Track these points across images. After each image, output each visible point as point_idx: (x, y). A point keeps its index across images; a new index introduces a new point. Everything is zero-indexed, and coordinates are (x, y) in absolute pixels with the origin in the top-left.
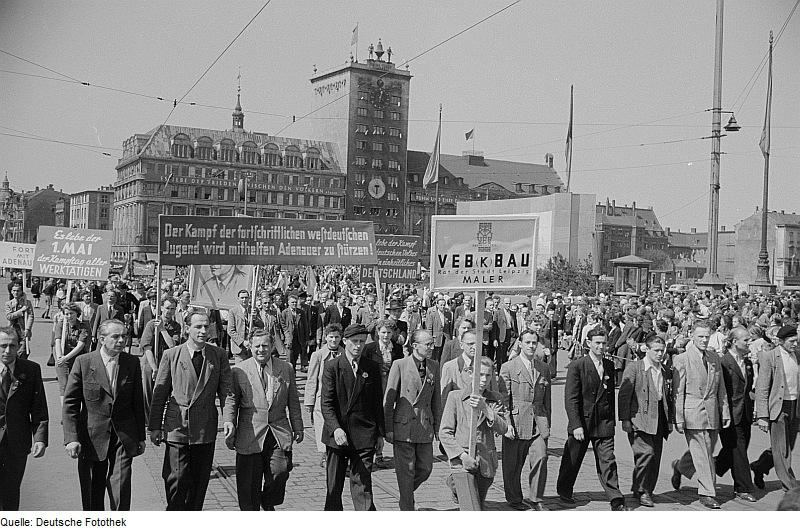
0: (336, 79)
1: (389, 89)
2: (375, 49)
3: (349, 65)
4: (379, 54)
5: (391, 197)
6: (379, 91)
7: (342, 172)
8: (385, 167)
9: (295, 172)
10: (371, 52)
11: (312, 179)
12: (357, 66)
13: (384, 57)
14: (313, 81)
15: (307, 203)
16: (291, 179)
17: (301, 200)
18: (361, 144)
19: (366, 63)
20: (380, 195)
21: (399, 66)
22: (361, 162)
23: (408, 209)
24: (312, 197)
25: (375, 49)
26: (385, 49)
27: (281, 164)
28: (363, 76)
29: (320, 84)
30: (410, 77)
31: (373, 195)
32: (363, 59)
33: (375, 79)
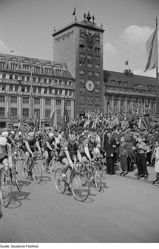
0: (68, 31)
1: (95, 36)
2: (87, 16)
3: (74, 23)
4: (89, 18)
5: (97, 91)
6: (89, 38)
7: (73, 77)
8: (93, 75)
9: (50, 77)
10: (85, 17)
11: (58, 80)
12: (79, 23)
13: (91, 20)
14: (54, 35)
15: (56, 93)
16: (48, 81)
17: (53, 91)
18: (81, 61)
19: (83, 22)
20: (91, 90)
21: (98, 26)
22: (82, 72)
23: (105, 97)
24: (59, 90)
25: (87, 16)
26: (91, 16)
27: (42, 72)
28: (83, 29)
29: (58, 36)
30: (102, 31)
31: (89, 89)
32: (80, 19)
33: (87, 31)
